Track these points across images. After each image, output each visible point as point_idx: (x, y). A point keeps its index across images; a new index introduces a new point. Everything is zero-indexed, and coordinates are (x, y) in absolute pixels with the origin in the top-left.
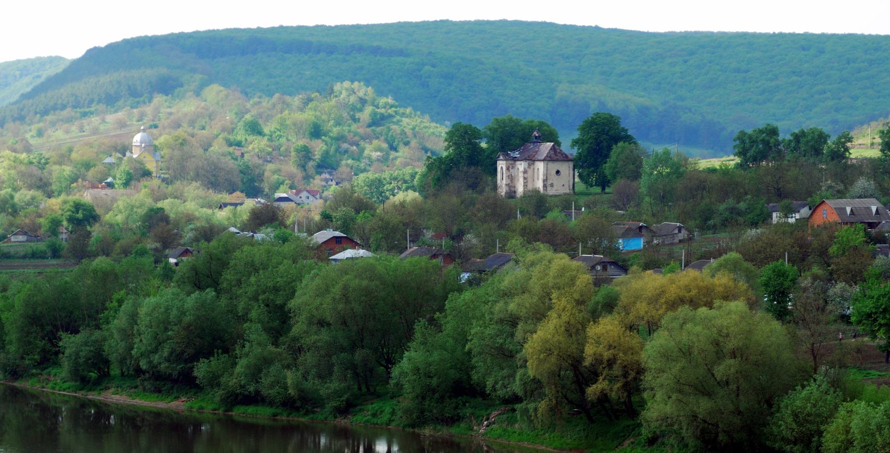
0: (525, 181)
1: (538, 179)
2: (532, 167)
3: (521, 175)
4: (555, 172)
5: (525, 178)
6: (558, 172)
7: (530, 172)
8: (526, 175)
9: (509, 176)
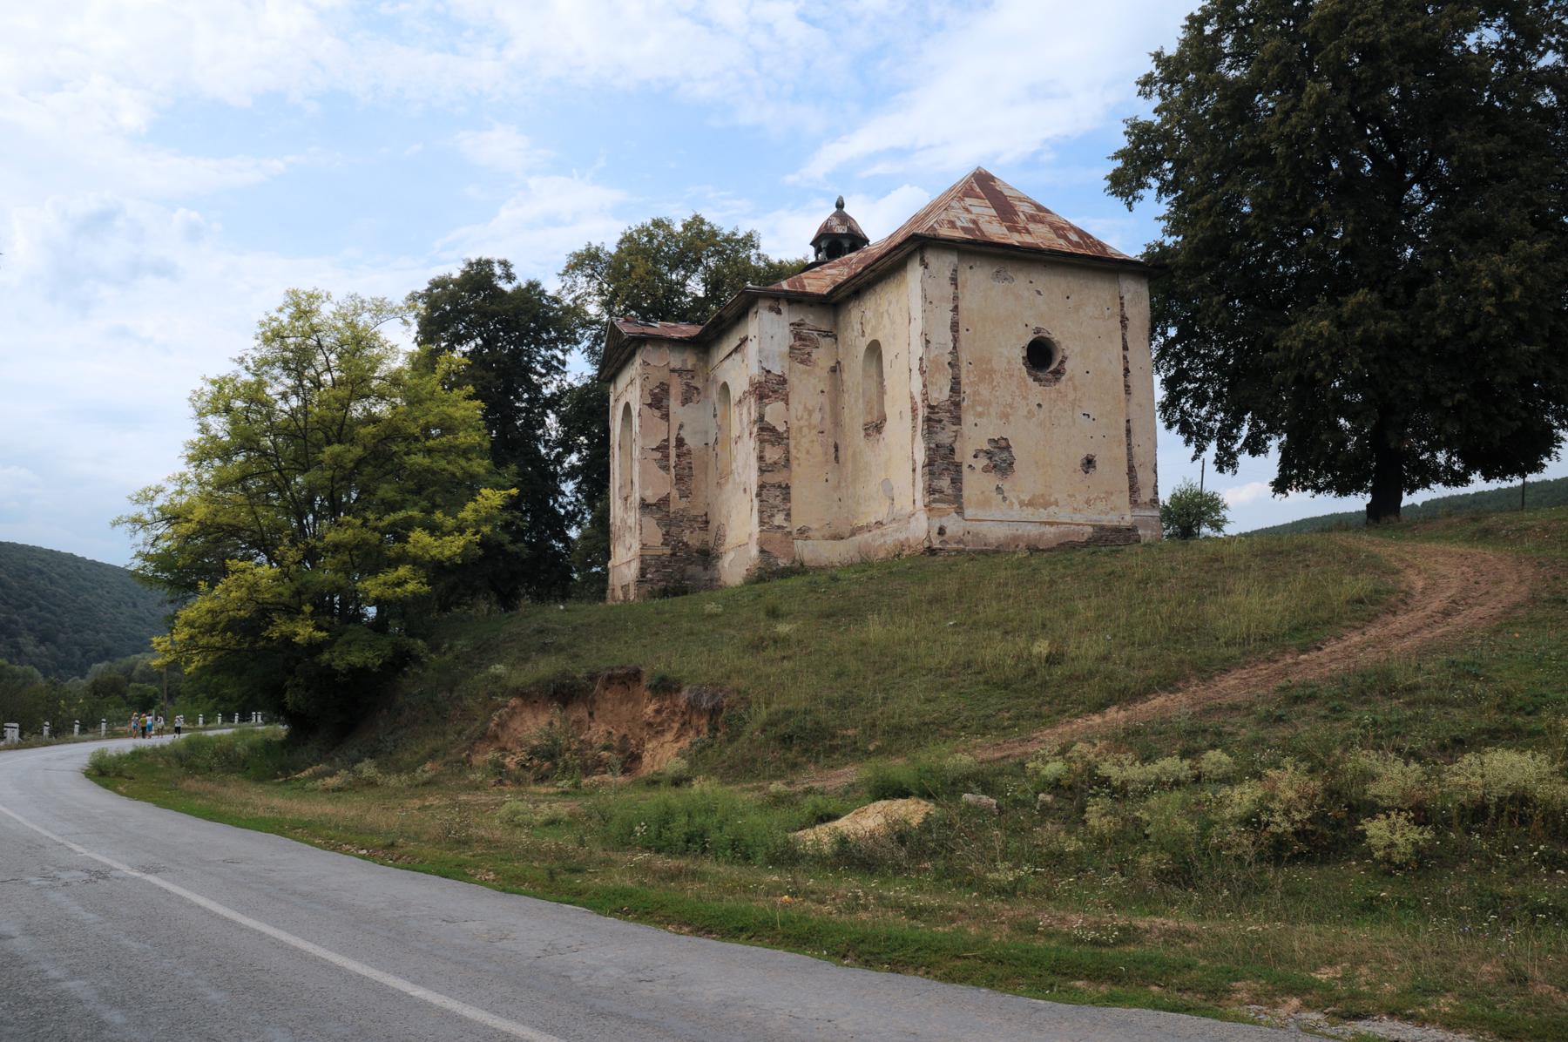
0: (773, 454)
1: (875, 427)
3: (741, 420)
4: (1019, 354)
5: (767, 433)
6: (1040, 355)
7: (807, 388)
8: (774, 412)
9: (663, 448)
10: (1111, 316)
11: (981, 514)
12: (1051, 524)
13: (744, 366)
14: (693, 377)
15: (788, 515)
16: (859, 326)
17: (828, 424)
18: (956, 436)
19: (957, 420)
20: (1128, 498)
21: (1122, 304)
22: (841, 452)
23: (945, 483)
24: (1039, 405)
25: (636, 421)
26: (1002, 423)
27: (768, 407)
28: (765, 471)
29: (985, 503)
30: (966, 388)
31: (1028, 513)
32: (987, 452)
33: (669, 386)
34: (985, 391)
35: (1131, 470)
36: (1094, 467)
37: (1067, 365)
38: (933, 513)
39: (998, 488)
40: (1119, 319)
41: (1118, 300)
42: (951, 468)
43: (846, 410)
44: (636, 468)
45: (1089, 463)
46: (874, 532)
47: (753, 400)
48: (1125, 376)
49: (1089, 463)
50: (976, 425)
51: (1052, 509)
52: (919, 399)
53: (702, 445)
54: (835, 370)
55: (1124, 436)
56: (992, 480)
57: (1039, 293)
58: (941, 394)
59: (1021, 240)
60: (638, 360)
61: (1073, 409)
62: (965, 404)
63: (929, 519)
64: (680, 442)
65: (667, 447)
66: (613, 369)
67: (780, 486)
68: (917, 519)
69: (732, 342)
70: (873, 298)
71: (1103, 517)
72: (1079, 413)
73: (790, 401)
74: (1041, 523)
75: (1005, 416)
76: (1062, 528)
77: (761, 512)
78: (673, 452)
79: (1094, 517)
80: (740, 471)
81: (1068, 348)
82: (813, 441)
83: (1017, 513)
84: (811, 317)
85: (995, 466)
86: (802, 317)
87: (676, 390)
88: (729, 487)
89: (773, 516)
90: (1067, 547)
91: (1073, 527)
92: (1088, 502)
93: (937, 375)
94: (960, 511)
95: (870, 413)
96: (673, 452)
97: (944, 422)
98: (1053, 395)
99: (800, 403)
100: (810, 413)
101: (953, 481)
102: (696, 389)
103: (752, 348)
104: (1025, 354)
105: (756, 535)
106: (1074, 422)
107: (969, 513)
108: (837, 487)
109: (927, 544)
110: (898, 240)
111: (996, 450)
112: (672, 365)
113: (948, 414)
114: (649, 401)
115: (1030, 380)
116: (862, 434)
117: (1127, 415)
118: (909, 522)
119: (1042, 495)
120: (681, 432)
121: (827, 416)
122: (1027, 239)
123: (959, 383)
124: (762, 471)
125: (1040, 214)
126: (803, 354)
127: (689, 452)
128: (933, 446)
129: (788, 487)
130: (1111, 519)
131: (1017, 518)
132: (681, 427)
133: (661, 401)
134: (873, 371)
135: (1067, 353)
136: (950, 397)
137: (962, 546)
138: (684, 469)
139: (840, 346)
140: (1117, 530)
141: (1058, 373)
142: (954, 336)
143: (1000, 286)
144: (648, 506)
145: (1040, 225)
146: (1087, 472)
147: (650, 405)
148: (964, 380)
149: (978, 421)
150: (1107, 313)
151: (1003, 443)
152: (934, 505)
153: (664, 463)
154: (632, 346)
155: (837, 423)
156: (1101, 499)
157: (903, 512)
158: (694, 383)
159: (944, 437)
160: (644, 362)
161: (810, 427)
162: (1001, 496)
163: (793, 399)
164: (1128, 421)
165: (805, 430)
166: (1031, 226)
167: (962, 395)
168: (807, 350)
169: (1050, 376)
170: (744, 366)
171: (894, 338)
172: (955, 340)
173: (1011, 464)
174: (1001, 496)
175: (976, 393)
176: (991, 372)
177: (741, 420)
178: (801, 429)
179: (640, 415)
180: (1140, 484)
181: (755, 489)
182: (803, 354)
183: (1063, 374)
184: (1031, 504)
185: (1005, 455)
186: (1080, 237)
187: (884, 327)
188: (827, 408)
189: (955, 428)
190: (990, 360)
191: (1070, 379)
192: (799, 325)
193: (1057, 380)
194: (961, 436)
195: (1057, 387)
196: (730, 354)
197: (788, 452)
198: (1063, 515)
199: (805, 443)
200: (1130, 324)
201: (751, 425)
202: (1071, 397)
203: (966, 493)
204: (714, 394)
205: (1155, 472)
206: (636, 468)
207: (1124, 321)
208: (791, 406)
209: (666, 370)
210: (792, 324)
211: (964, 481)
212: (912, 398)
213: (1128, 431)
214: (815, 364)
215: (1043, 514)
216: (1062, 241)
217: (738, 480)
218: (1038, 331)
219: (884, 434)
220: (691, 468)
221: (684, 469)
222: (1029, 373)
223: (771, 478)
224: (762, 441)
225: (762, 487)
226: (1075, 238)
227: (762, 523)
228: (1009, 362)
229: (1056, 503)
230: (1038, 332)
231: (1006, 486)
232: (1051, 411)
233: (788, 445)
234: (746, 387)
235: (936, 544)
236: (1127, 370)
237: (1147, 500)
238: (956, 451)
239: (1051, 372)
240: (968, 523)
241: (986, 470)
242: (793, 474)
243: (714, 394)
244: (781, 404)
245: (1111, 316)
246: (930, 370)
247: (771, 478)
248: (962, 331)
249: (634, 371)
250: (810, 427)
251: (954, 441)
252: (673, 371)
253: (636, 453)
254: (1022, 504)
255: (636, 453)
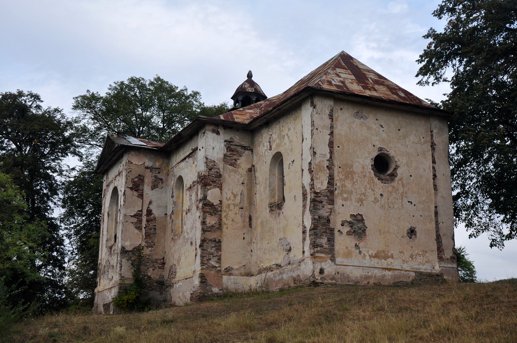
0: (211, 221)
2: (243, 162)
4: (369, 163)
8: (213, 195)
9: (138, 215)
10: (425, 142)
11: (346, 261)
12: (390, 270)
13: (194, 166)
14: (159, 173)
15: (219, 259)
16: (268, 144)
17: (245, 204)
18: (331, 212)
19: (332, 202)
20: (437, 255)
21: (432, 136)
22: (254, 221)
23: (324, 241)
24: (381, 195)
25: (121, 199)
26: (358, 205)
27: (209, 192)
28: (206, 231)
29: (348, 255)
30: (338, 183)
31: (375, 262)
32: (350, 223)
33: (144, 177)
34: (348, 184)
35: (438, 238)
36: (415, 235)
37: (399, 171)
38: (317, 259)
39: (356, 245)
40: (430, 144)
41: (430, 133)
42: (328, 231)
43: (258, 196)
44: (120, 227)
45: (412, 232)
46: (275, 271)
47: (199, 187)
48: (434, 179)
49: (412, 232)
50: (343, 205)
51: (390, 260)
52: (308, 188)
53: (163, 215)
54: (251, 170)
55: (433, 216)
56: (351, 241)
57: (382, 126)
58: (322, 185)
59: (371, 94)
60: (125, 160)
61: (402, 199)
62: (336, 192)
63: (313, 263)
64: (149, 212)
65: (141, 215)
66: (107, 166)
67: (215, 241)
68: (306, 264)
69: (187, 150)
70: (278, 127)
71: (421, 266)
72: (405, 201)
73: (223, 188)
74: (383, 269)
75: (361, 201)
76: (396, 272)
77: (202, 257)
78: (144, 219)
79: (416, 267)
80: (189, 231)
81: (399, 160)
82: (236, 214)
83: (367, 262)
84: (238, 138)
85: (354, 232)
86: (232, 136)
87: (148, 179)
88: (180, 241)
89: (210, 259)
90: (398, 285)
91: (403, 272)
92: (411, 256)
93: (320, 174)
94: (333, 259)
95: (273, 197)
96: (144, 219)
97: (324, 203)
98: (390, 189)
99: (229, 189)
100: (235, 196)
101: (329, 240)
102: (161, 180)
103: (200, 155)
104: (373, 163)
105: (198, 272)
106: (402, 205)
107: (338, 260)
108: (250, 243)
109: (312, 279)
110: (292, 93)
111: (355, 222)
112: (146, 165)
113: (326, 198)
114: (131, 186)
115: (376, 180)
116: (268, 210)
117: (435, 203)
118: (300, 265)
119: (383, 251)
120: (150, 206)
121: (245, 198)
122: (374, 94)
123: (333, 179)
124: (204, 231)
125: (381, 80)
126: (232, 160)
127: (155, 219)
128: (317, 217)
129: (220, 241)
130: (426, 268)
131: (367, 265)
132: (150, 203)
133: (138, 186)
134: (276, 171)
135: (399, 163)
136: (328, 187)
137: (334, 281)
138: (151, 229)
139: (255, 157)
140: (430, 275)
141: (393, 176)
142: (330, 150)
143: (358, 121)
144: (127, 252)
145: (381, 87)
146: (410, 238)
147: (131, 188)
148: (336, 178)
149: (344, 203)
150: (423, 140)
151: (359, 218)
152: (317, 255)
153: (139, 225)
154: (121, 152)
155: (251, 203)
156: (420, 255)
157: (296, 259)
158: (159, 176)
159: (324, 212)
160: (129, 161)
161: (235, 205)
162: (358, 251)
163: (225, 187)
164: (436, 207)
165: (232, 207)
166: (376, 87)
167: (335, 187)
168: (235, 157)
169: (388, 177)
170: (194, 166)
171: (291, 152)
172: (331, 153)
173: (364, 231)
174: (358, 251)
175: (343, 186)
176: (352, 173)
177: (190, 199)
178: (229, 206)
179: (124, 194)
180: (444, 247)
181: (199, 243)
182: (232, 160)
183: (396, 176)
184: (376, 256)
185: (360, 225)
186: (405, 94)
187: (285, 144)
188: (245, 193)
189: (330, 207)
190: (352, 166)
191: (400, 180)
192: (230, 142)
193: (392, 180)
194: (334, 212)
195: (392, 184)
196: (185, 159)
197: (221, 220)
198: (396, 264)
199: (231, 215)
200: (437, 148)
201: (198, 203)
202: (401, 190)
203: (337, 247)
204: (172, 182)
205: (453, 239)
206: (120, 227)
207: (433, 146)
208: (223, 192)
209: (143, 167)
210: (225, 141)
211: (336, 240)
212: (303, 187)
213: (436, 213)
214: (239, 166)
215: (384, 263)
216: (395, 96)
217: (187, 237)
218: (381, 149)
219: (283, 210)
220: (155, 229)
221: (151, 229)
222: (375, 175)
223: (211, 236)
224: (204, 212)
225: (203, 241)
226: (403, 95)
227: (202, 264)
228: (363, 168)
229: (392, 257)
230: (381, 150)
231: (361, 245)
232: (388, 199)
233: (221, 215)
234: (195, 178)
235: (318, 278)
236: (435, 176)
237: (449, 257)
238: (331, 221)
239: (388, 175)
240: (338, 267)
241: (349, 233)
242: (223, 233)
243: (172, 182)
244: (217, 190)
245: (425, 142)
246: (316, 170)
247: (211, 236)
248: (336, 148)
249: (121, 167)
250: (235, 205)
251: (330, 215)
252: (147, 168)
253: (121, 218)
254: (371, 257)
255: (121, 218)
